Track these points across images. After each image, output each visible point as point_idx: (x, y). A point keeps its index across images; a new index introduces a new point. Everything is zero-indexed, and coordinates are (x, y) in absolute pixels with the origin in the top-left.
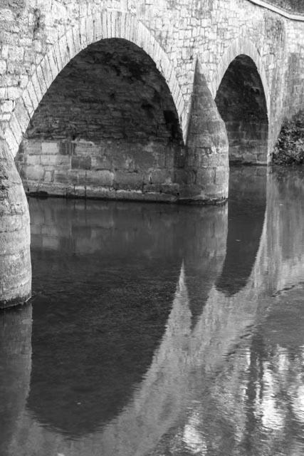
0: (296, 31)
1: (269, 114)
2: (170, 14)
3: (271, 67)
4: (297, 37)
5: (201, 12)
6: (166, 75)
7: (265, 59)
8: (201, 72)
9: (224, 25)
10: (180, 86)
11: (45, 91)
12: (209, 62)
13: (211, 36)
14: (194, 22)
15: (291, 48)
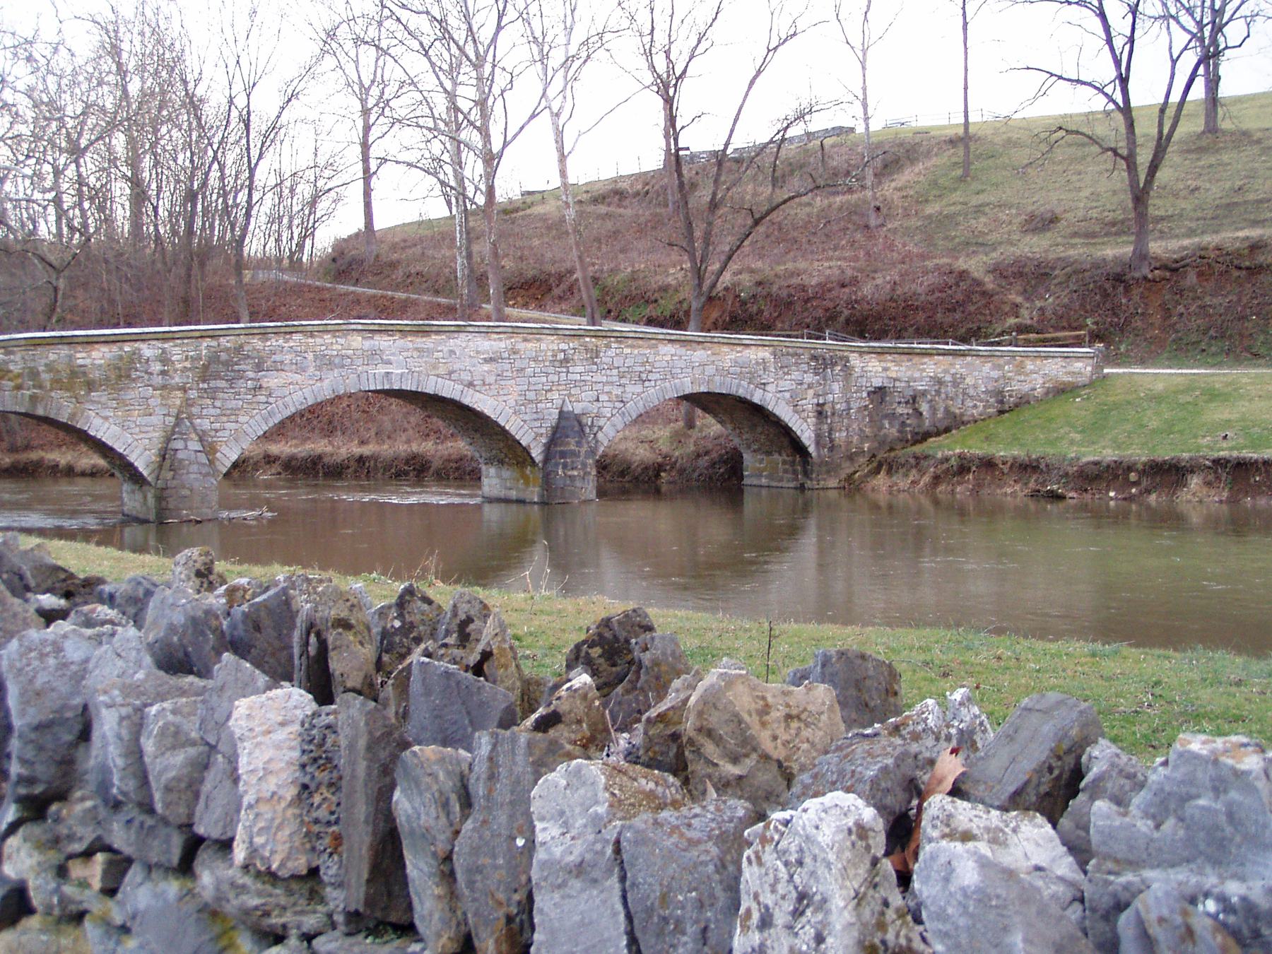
0: (883, 364)
1: (812, 449)
2: (486, 367)
3: (809, 403)
4: (886, 369)
5: (566, 360)
6: (488, 412)
7: (787, 395)
8: (565, 409)
9: (642, 369)
10: (525, 421)
11: (271, 424)
12: (598, 400)
13: (598, 377)
14: (551, 370)
15: (877, 382)
